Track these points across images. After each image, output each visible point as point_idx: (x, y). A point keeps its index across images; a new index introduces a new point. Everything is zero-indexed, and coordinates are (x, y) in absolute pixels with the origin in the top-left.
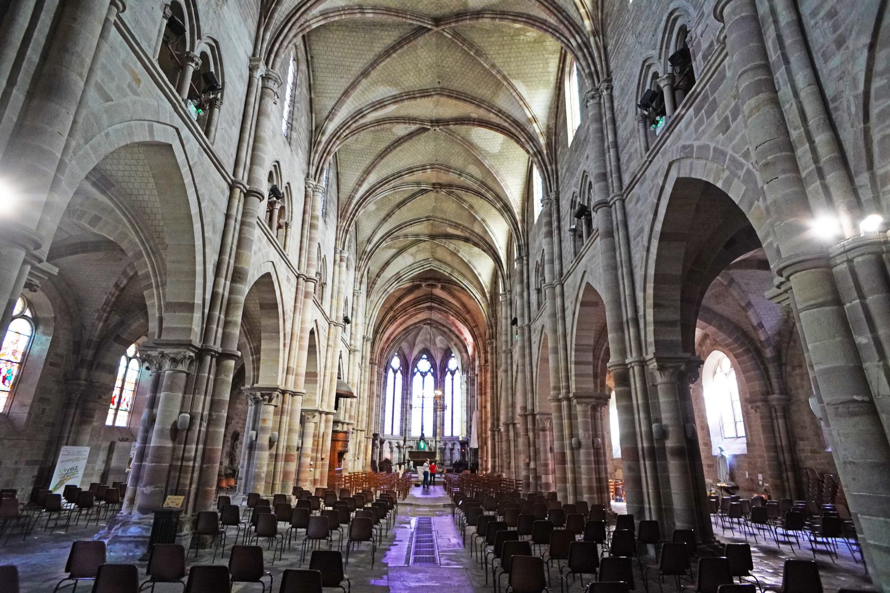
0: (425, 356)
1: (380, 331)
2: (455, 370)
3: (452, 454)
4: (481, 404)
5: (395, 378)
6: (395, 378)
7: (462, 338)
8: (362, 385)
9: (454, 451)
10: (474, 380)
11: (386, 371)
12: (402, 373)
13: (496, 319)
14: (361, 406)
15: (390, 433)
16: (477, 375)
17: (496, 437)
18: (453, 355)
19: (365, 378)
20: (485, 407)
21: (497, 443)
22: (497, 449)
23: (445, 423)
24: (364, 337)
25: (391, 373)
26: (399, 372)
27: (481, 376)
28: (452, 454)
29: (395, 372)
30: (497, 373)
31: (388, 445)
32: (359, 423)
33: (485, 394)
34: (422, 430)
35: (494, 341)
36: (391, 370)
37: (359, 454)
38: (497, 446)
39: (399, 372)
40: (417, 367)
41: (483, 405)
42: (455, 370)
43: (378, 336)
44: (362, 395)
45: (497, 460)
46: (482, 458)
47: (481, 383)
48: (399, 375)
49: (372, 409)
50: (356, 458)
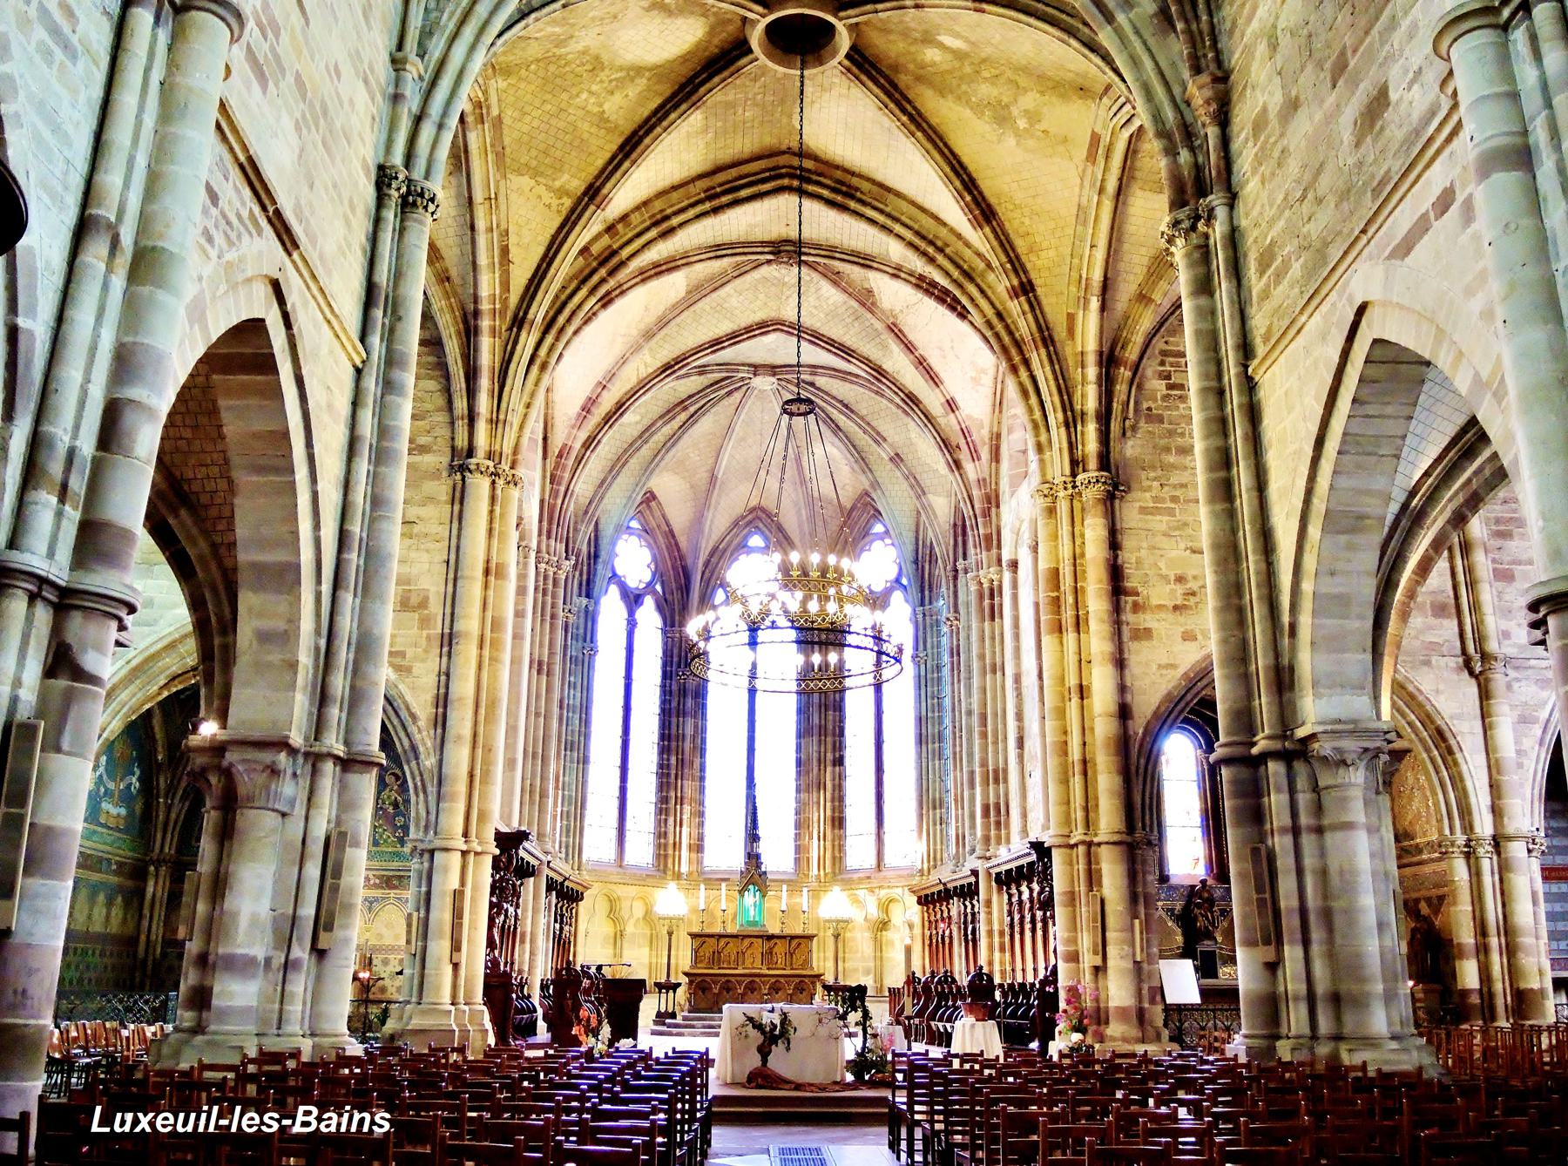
0: (756, 541)
1: (539, 311)
2: (888, 592)
3: (879, 945)
4: (1062, 680)
5: (632, 625)
6: (632, 625)
7: (932, 400)
8: (363, 467)
9: (888, 935)
10: (994, 592)
11: (588, 589)
12: (659, 608)
13: (1223, 78)
14: (348, 600)
15: (608, 852)
16: (1014, 565)
17: (1276, 802)
18: (878, 528)
19: (383, 431)
20: (1083, 692)
21: (1281, 844)
22: (1287, 885)
23: (849, 813)
24: (383, 177)
25: (611, 607)
26: (649, 602)
27: (1055, 537)
28: (879, 945)
29: (633, 600)
30: (1250, 385)
31: (603, 907)
32: (335, 713)
33: (1079, 624)
34: (753, 837)
35: (1216, 199)
36: (614, 590)
37: (324, 922)
38: (1285, 862)
39: (649, 602)
40: (724, 585)
41: (1072, 681)
42: (888, 592)
43: (528, 340)
44: (356, 528)
45: (1292, 954)
46: (1074, 957)
47: (1055, 574)
48: (649, 616)
49: (493, 704)
50: (301, 952)
